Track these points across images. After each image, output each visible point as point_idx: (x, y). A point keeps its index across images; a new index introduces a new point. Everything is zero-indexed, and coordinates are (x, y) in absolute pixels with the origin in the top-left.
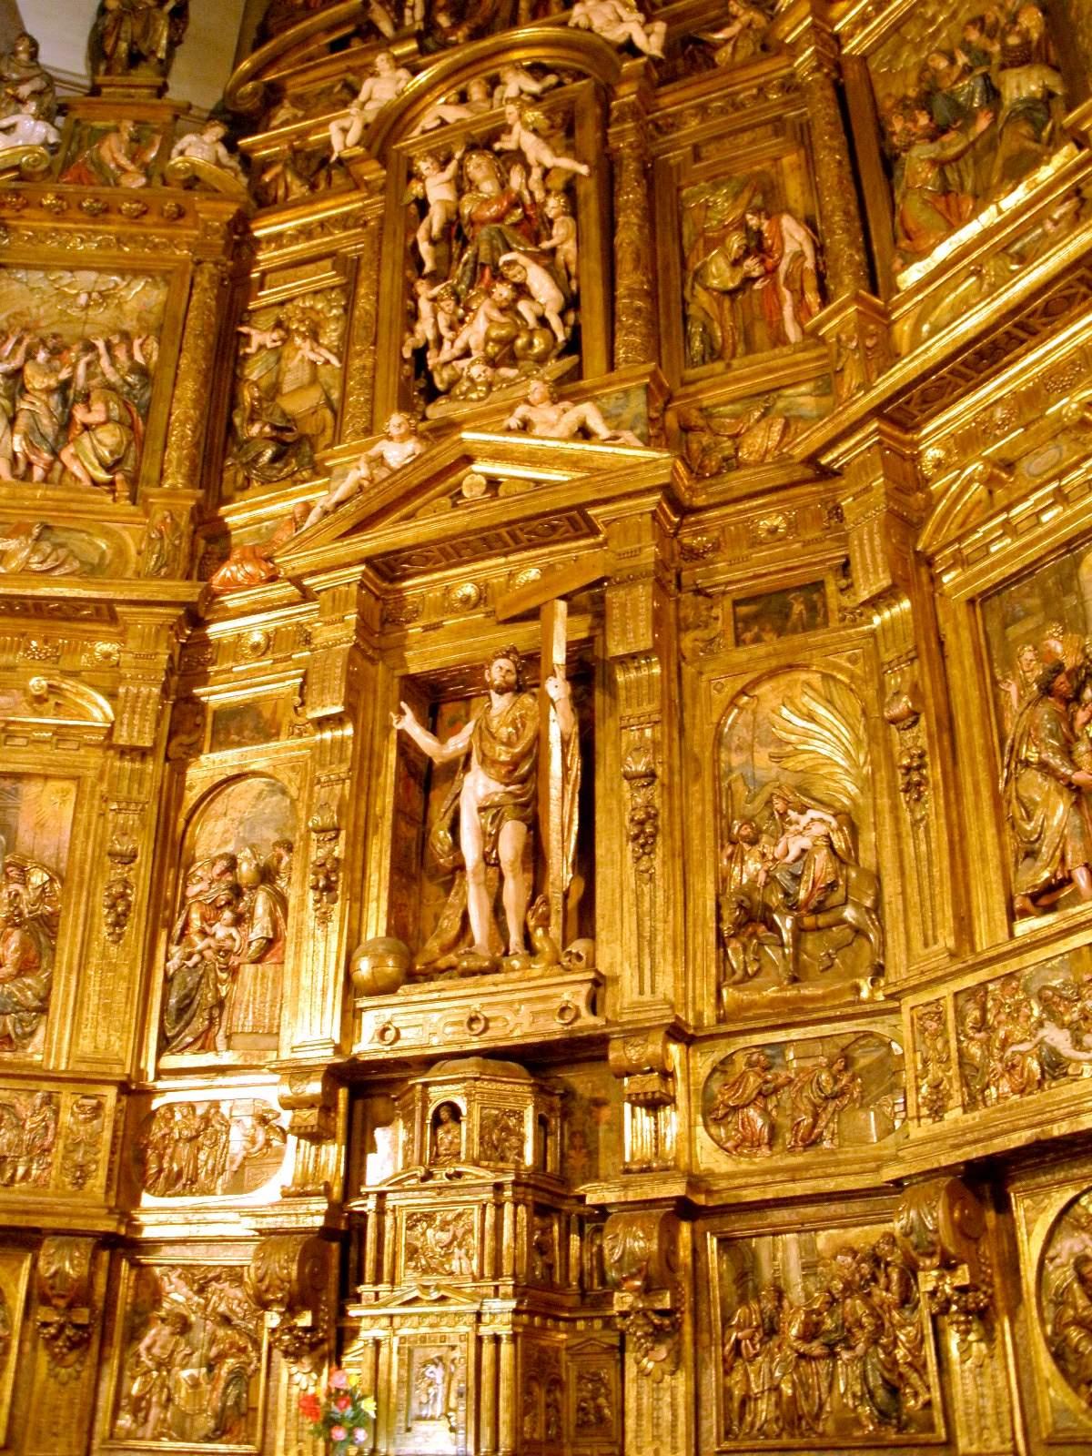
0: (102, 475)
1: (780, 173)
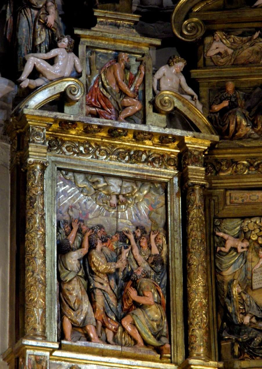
0: (152, 340)
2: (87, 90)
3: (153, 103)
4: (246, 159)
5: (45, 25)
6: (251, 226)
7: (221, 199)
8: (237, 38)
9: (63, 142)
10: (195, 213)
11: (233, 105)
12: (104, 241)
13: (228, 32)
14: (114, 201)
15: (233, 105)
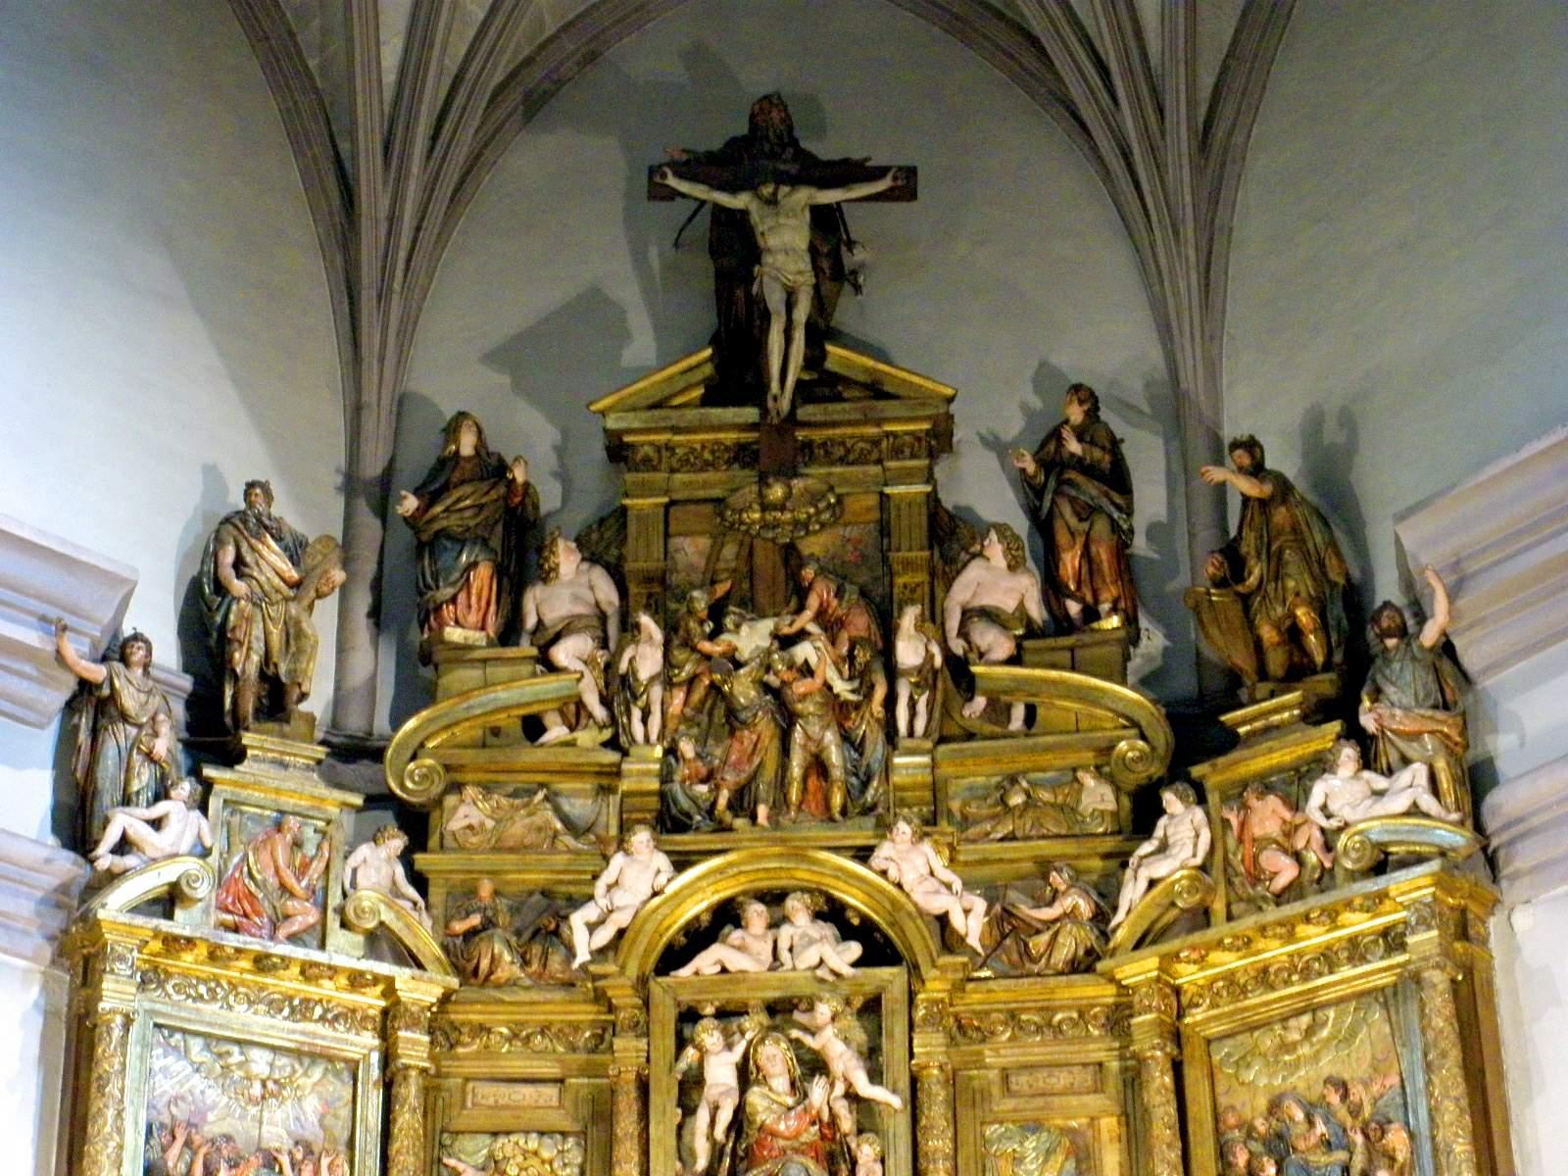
1: (1097, 1137)
2: (221, 881)
3: (341, 911)
4: (506, 1024)
5: (149, 757)
6: (509, 1150)
7: (457, 1097)
8: (504, 801)
9: (169, 975)
10: (407, 1119)
11: (488, 924)
12: (234, 1165)
13: (487, 789)
14: (256, 1090)
15: (488, 924)
